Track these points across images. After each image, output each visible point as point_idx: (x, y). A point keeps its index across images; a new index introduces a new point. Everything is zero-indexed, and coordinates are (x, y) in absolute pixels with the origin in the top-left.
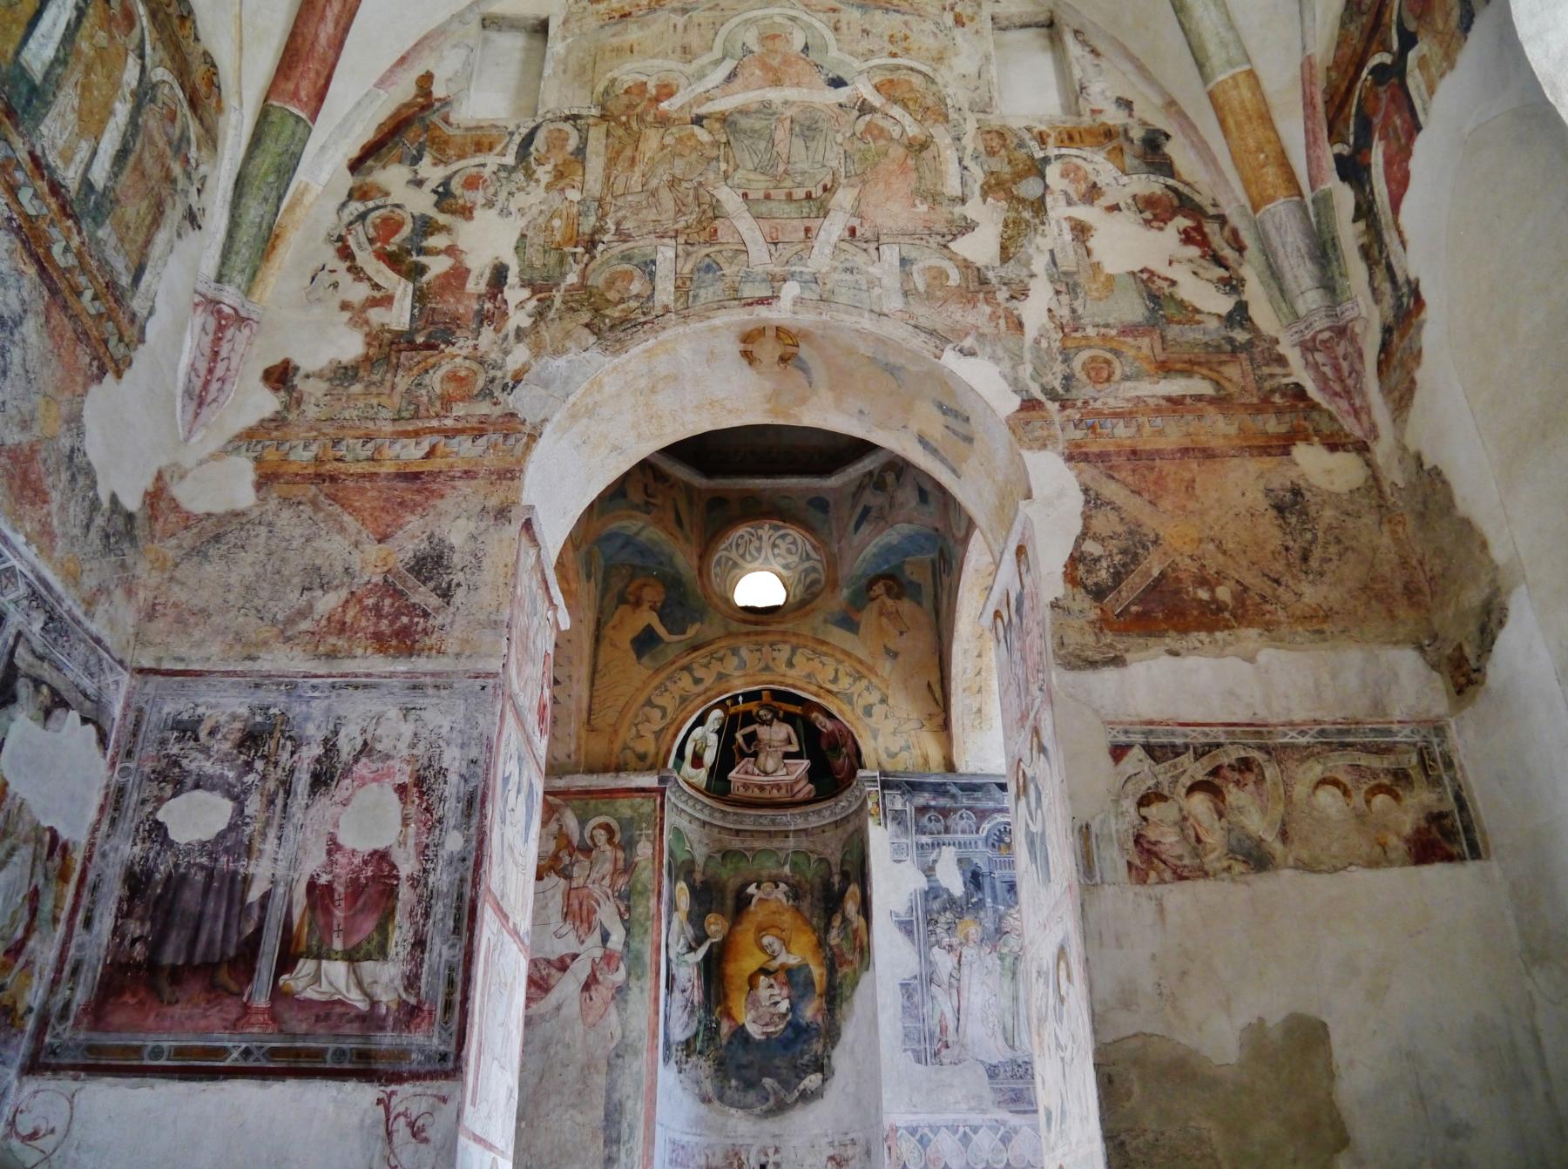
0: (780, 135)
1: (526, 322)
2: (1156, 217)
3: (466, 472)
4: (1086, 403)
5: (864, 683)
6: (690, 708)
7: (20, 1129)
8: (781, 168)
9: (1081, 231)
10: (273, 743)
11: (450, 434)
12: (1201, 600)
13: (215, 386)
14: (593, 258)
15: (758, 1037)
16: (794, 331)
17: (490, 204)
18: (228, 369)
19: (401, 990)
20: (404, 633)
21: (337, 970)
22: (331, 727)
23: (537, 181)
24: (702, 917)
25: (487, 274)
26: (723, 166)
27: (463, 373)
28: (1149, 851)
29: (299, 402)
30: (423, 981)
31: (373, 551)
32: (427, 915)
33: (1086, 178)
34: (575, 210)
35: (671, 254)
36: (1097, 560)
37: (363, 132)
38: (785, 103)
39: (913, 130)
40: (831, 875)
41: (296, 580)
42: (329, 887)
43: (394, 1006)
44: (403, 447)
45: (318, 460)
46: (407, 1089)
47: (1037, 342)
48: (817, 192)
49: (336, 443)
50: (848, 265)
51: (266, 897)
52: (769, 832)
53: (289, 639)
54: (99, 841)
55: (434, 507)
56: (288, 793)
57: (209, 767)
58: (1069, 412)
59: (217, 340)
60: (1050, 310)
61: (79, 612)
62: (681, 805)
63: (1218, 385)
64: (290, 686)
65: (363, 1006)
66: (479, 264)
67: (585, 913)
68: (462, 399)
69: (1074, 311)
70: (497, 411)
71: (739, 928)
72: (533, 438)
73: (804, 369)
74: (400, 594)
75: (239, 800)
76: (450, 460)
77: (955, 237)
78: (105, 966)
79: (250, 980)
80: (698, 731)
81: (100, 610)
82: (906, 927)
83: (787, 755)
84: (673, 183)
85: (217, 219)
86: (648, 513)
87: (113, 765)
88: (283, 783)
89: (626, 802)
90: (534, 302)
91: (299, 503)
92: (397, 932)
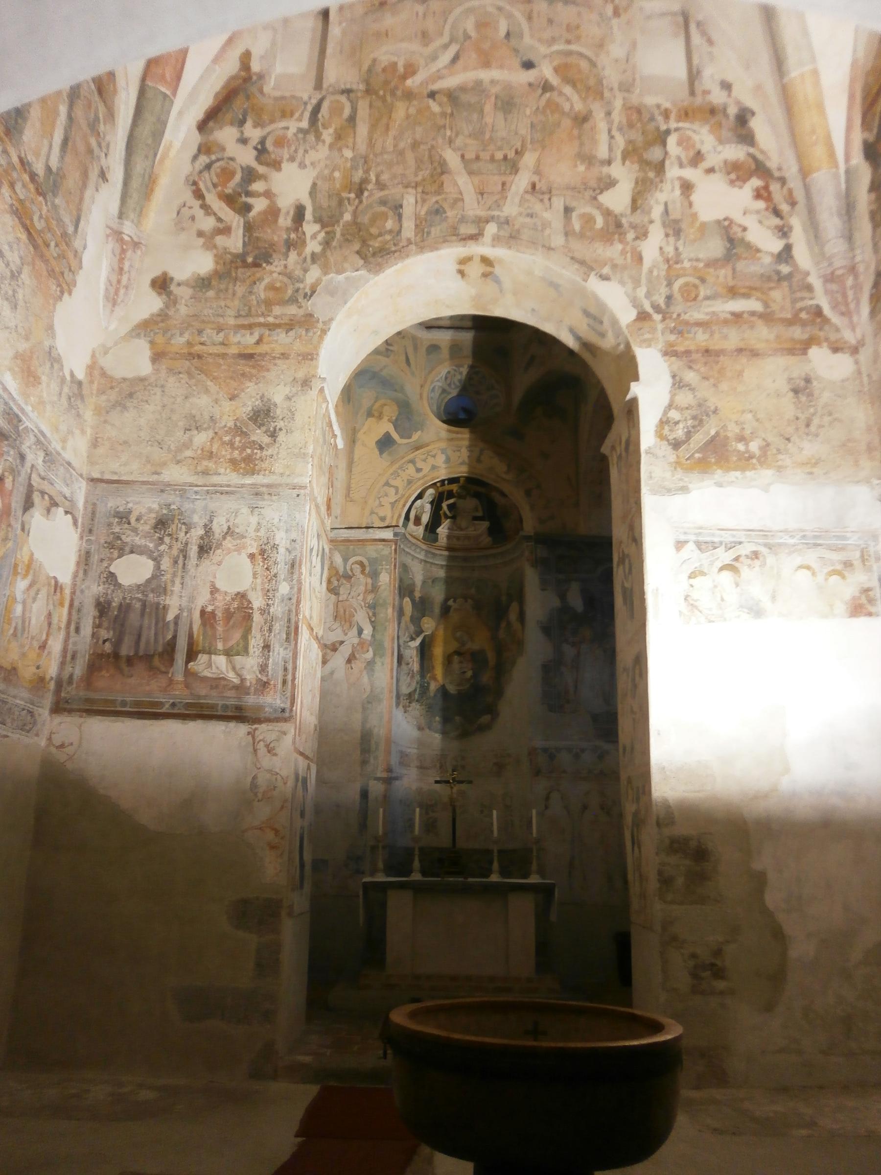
0: (488, 108)
1: (318, 249)
2: (738, 178)
3: (283, 354)
4: (679, 315)
6: (413, 488)
7: (54, 742)
8: (487, 136)
9: (687, 187)
10: (174, 527)
11: (272, 327)
12: (739, 451)
13: (122, 291)
14: (361, 202)
16: (492, 258)
17: (292, 159)
18: (129, 279)
19: (258, 672)
20: (248, 459)
21: (221, 661)
22: (208, 517)
23: (324, 142)
24: (420, 619)
25: (292, 213)
26: (448, 133)
27: (278, 285)
28: (692, 605)
29: (175, 302)
30: (270, 668)
31: (227, 406)
32: (270, 630)
33: (694, 146)
34: (349, 165)
35: (412, 200)
36: (677, 423)
37: (205, 101)
38: (492, 82)
39: (579, 106)
41: (181, 424)
42: (213, 613)
43: (254, 682)
44: (244, 335)
45: (189, 344)
46: (263, 727)
47: (651, 271)
48: (511, 155)
49: (200, 332)
50: (529, 211)
51: (177, 618)
53: (178, 462)
54: (78, 583)
55: (264, 377)
56: (185, 557)
57: (138, 541)
58: (667, 321)
59: (121, 260)
60: (661, 248)
61: (59, 448)
62: (407, 550)
63: (766, 305)
64: (182, 490)
65: (236, 681)
66: (286, 203)
67: (347, 616)
68: (278, 304)
69: (676, 249)
70: (301, 312)
72: (324, 332)
73: (497, 281)
74: (244, 434)
75: (157, 560)
76: (273, 345)
77: (601, 193)
78: (90, 655)
79: (172, 665)
80: (419, 502)
81: (70, 444)
82: (546, 630)
83: (475, 518)
84: (415, 145)
85: (117, 174)
86: (388, 357)
87: (81, 538)
88: (182, 551)
90: (323, 234)
91: (180, 373)
92: (253, 640)
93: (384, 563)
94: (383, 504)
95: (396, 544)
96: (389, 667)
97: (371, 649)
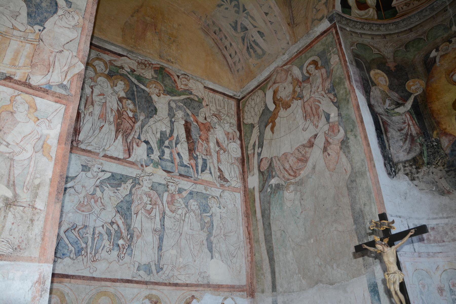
71: (433, 80)
89: (319, 44)
94: (318, 9)
97: (341, 129)
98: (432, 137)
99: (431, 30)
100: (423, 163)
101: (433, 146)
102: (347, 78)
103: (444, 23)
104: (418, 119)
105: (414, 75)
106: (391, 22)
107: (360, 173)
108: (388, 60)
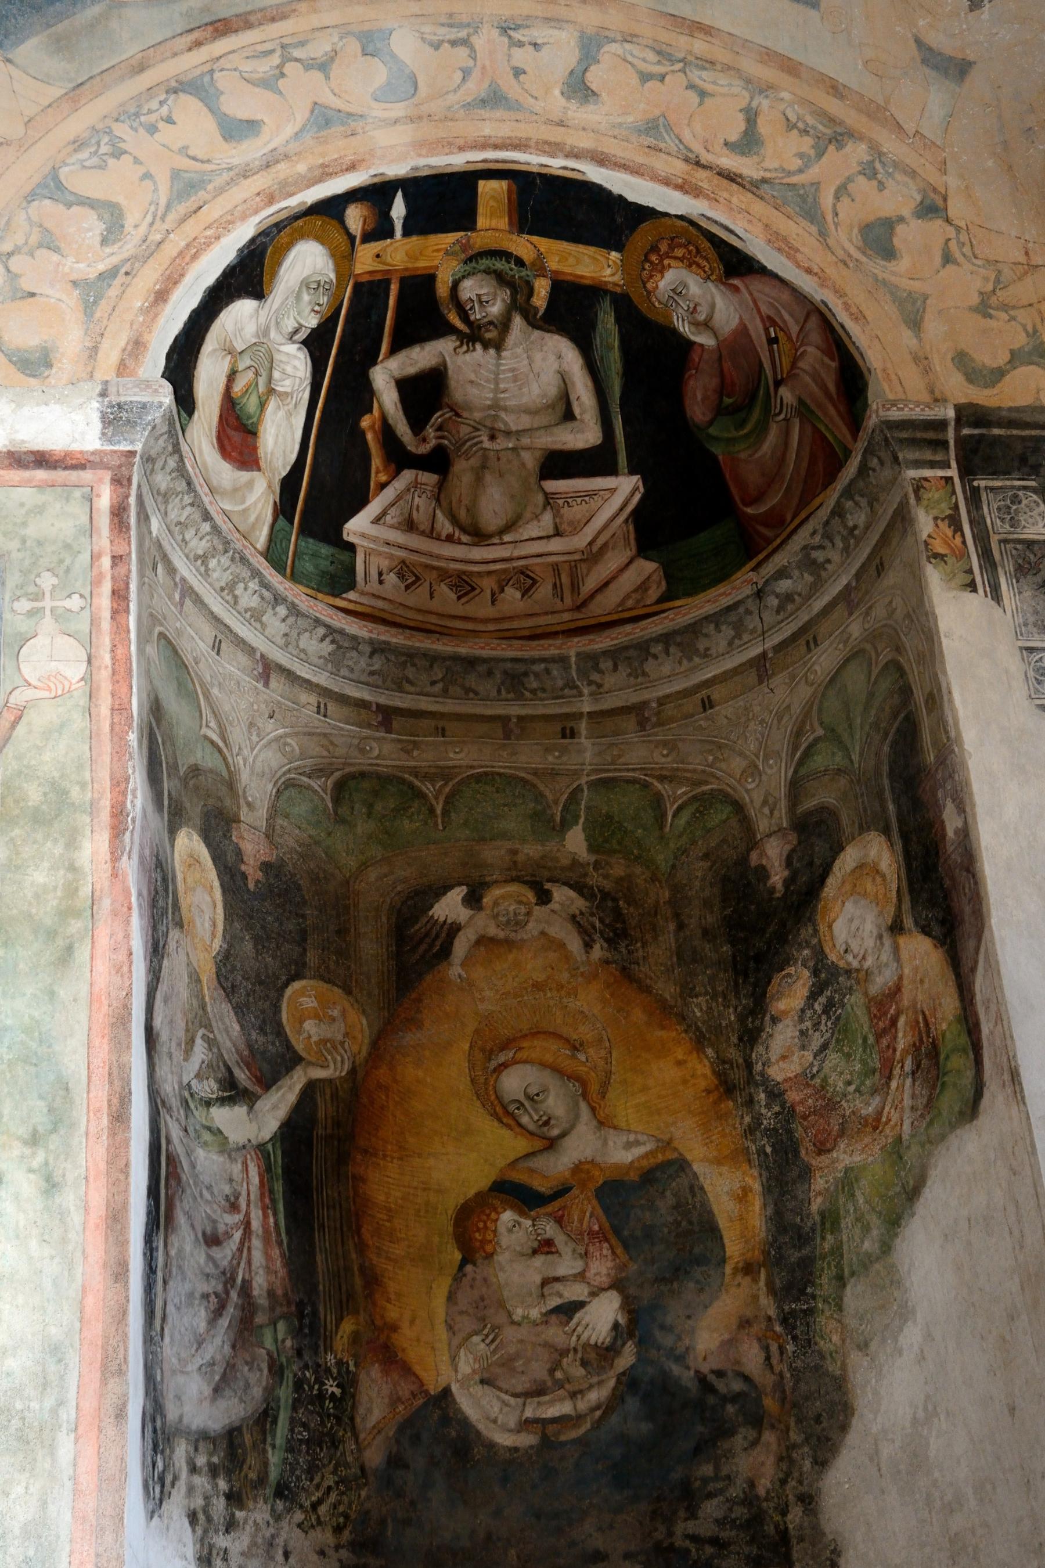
5: (857, 152)
6: (214, 211)
15: (504, 1439)
40: (751, 841)
52: (504, 720)
71: (410, 1038)
93: (47, 581)
95: (120, 481)
96: (98, 1198)
98: (329, 1348)
99: (479, 778)
100: (262, 1480)
101: (321, 1396)
102: (105, 816)
103: (541, 787)
104: (291, 1215)
105: (332, 966)
106: (328, 620)
107: (16, 1423)
108: (244, 814)
